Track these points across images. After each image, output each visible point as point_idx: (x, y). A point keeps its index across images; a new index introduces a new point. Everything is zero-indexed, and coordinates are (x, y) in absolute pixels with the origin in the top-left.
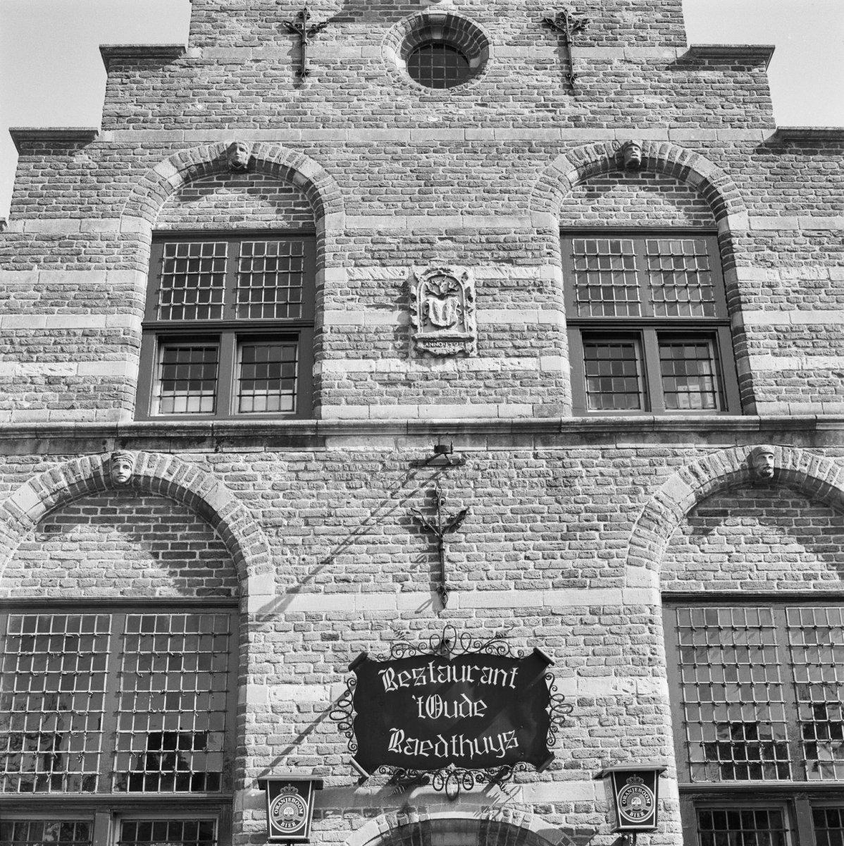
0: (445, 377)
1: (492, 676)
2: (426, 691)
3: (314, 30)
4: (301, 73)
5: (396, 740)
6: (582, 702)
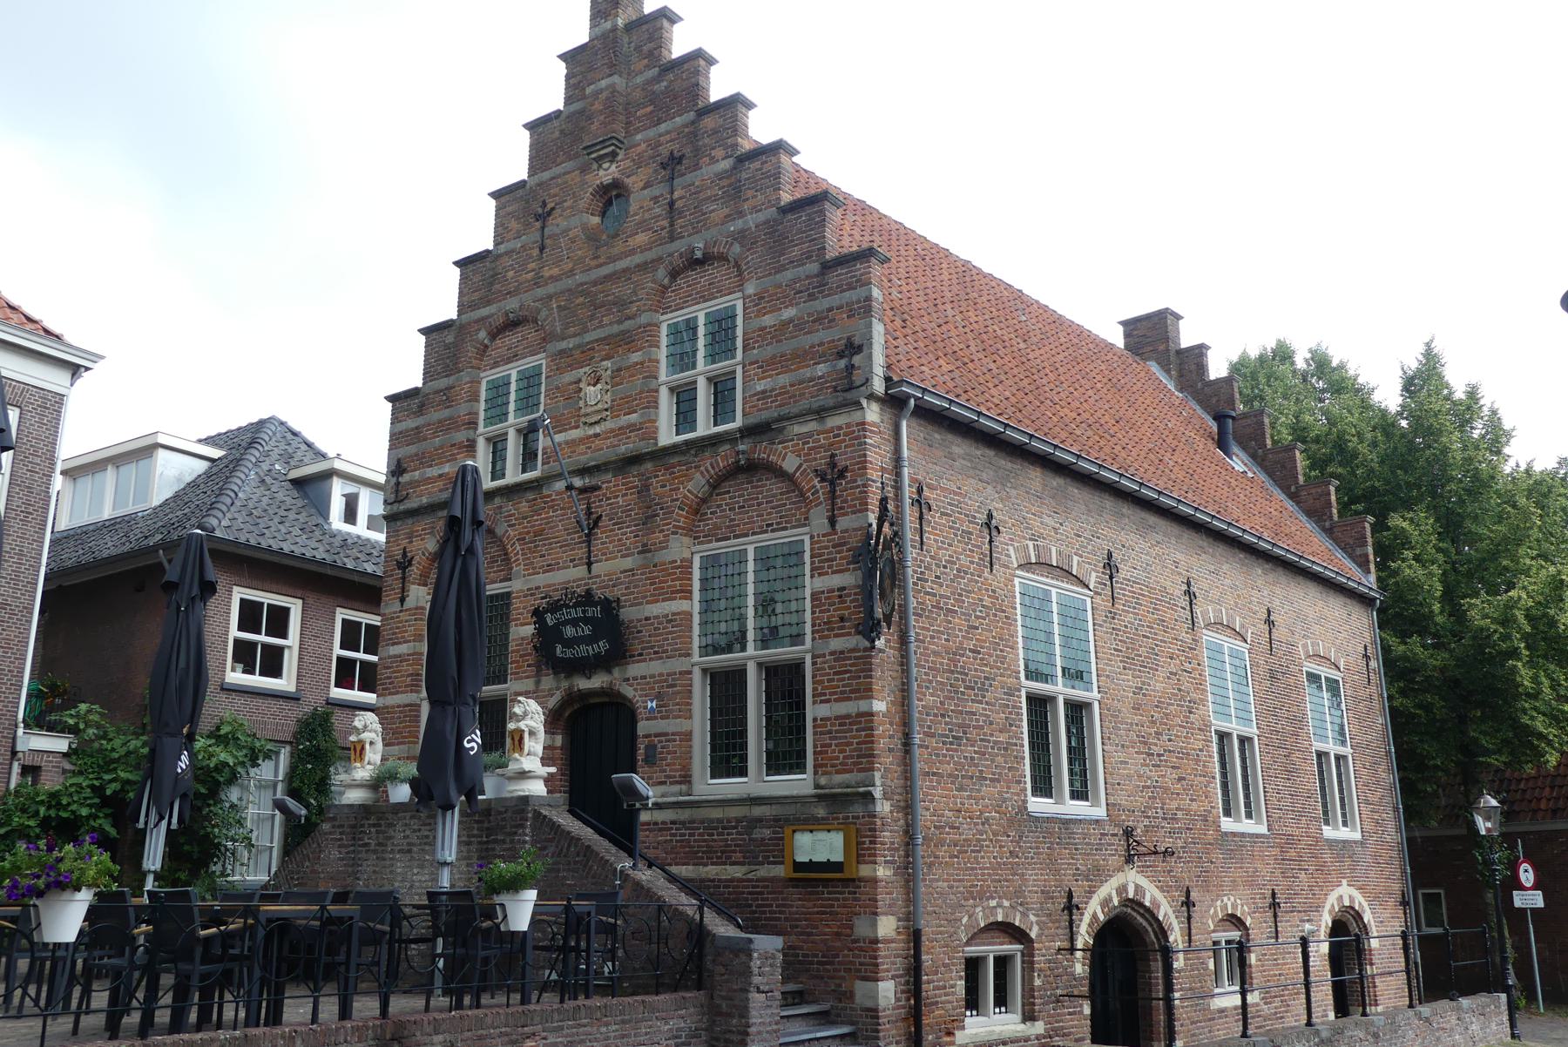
0: (596, 435)
1: (592, 612)
2: (566, 623)
3: (549, 213)
4: (542, 249)
5: (559, 648)
6: (647, 619)
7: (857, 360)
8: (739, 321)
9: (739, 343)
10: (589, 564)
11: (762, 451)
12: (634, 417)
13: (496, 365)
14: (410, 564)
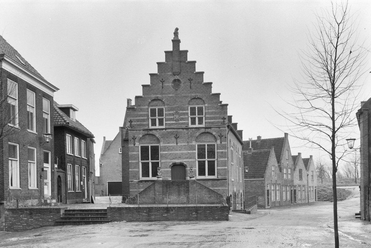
3: (164, 81)
4: (163, 88)
7: (225, 120)
8: (204, 109)
9: (204, 113)
10: (177, 144)
11: (209, 130)
12: (185, 122)
13: (152, 106)
14: (136, 138)
